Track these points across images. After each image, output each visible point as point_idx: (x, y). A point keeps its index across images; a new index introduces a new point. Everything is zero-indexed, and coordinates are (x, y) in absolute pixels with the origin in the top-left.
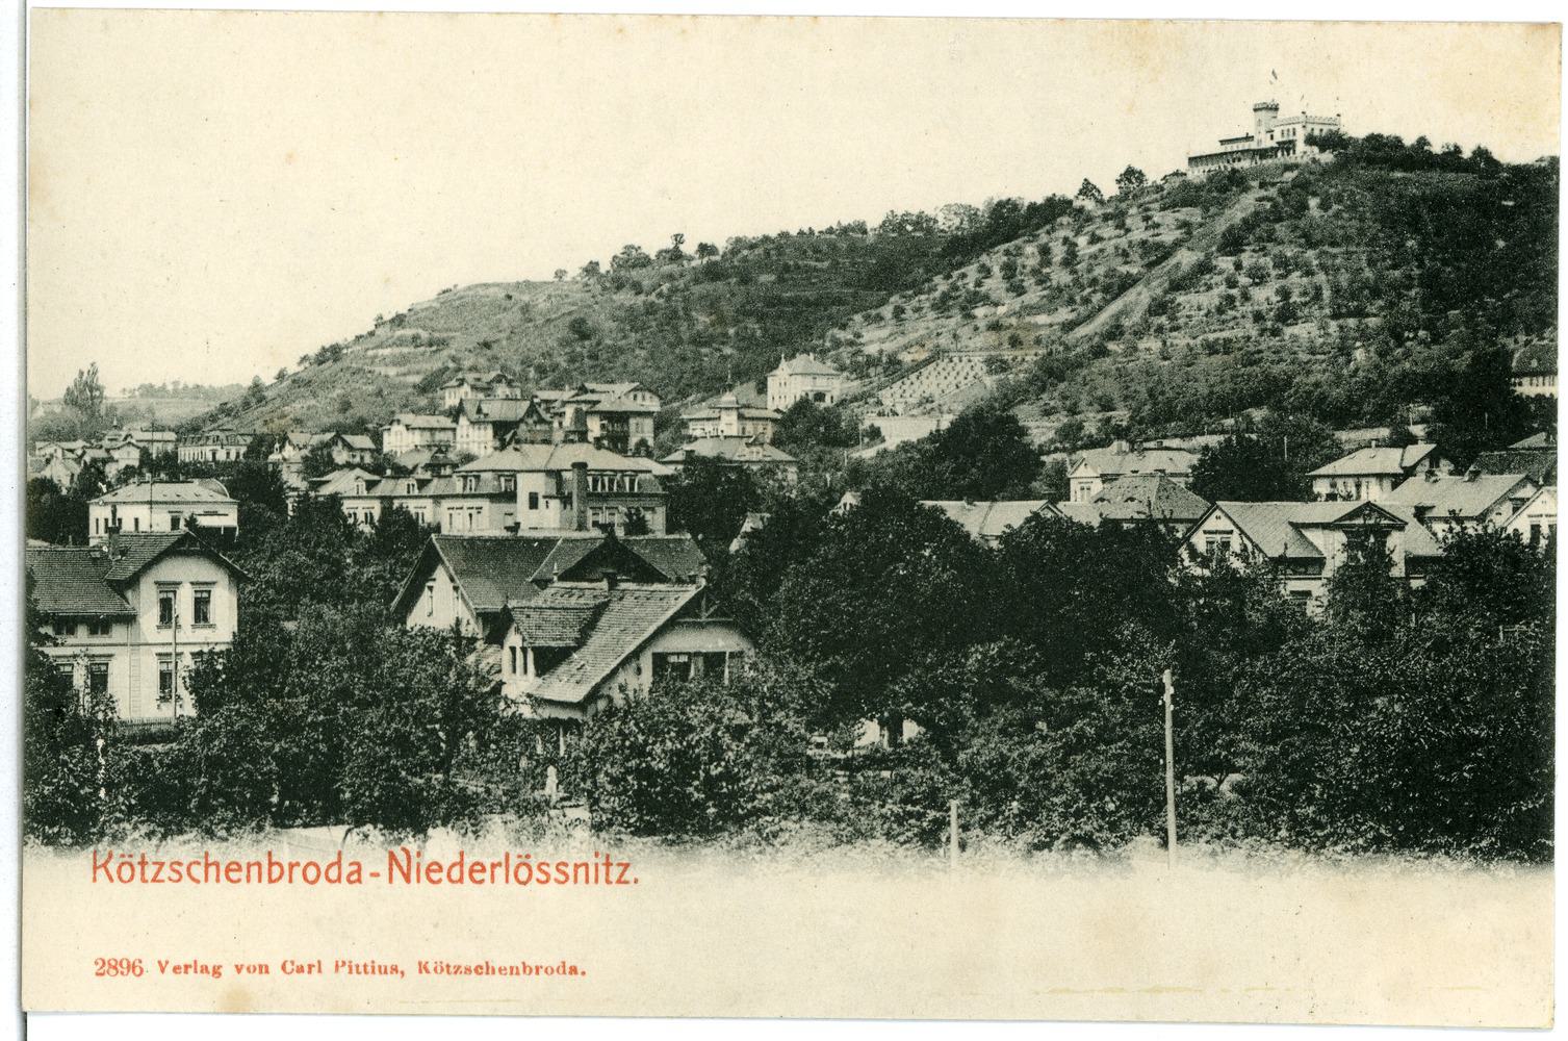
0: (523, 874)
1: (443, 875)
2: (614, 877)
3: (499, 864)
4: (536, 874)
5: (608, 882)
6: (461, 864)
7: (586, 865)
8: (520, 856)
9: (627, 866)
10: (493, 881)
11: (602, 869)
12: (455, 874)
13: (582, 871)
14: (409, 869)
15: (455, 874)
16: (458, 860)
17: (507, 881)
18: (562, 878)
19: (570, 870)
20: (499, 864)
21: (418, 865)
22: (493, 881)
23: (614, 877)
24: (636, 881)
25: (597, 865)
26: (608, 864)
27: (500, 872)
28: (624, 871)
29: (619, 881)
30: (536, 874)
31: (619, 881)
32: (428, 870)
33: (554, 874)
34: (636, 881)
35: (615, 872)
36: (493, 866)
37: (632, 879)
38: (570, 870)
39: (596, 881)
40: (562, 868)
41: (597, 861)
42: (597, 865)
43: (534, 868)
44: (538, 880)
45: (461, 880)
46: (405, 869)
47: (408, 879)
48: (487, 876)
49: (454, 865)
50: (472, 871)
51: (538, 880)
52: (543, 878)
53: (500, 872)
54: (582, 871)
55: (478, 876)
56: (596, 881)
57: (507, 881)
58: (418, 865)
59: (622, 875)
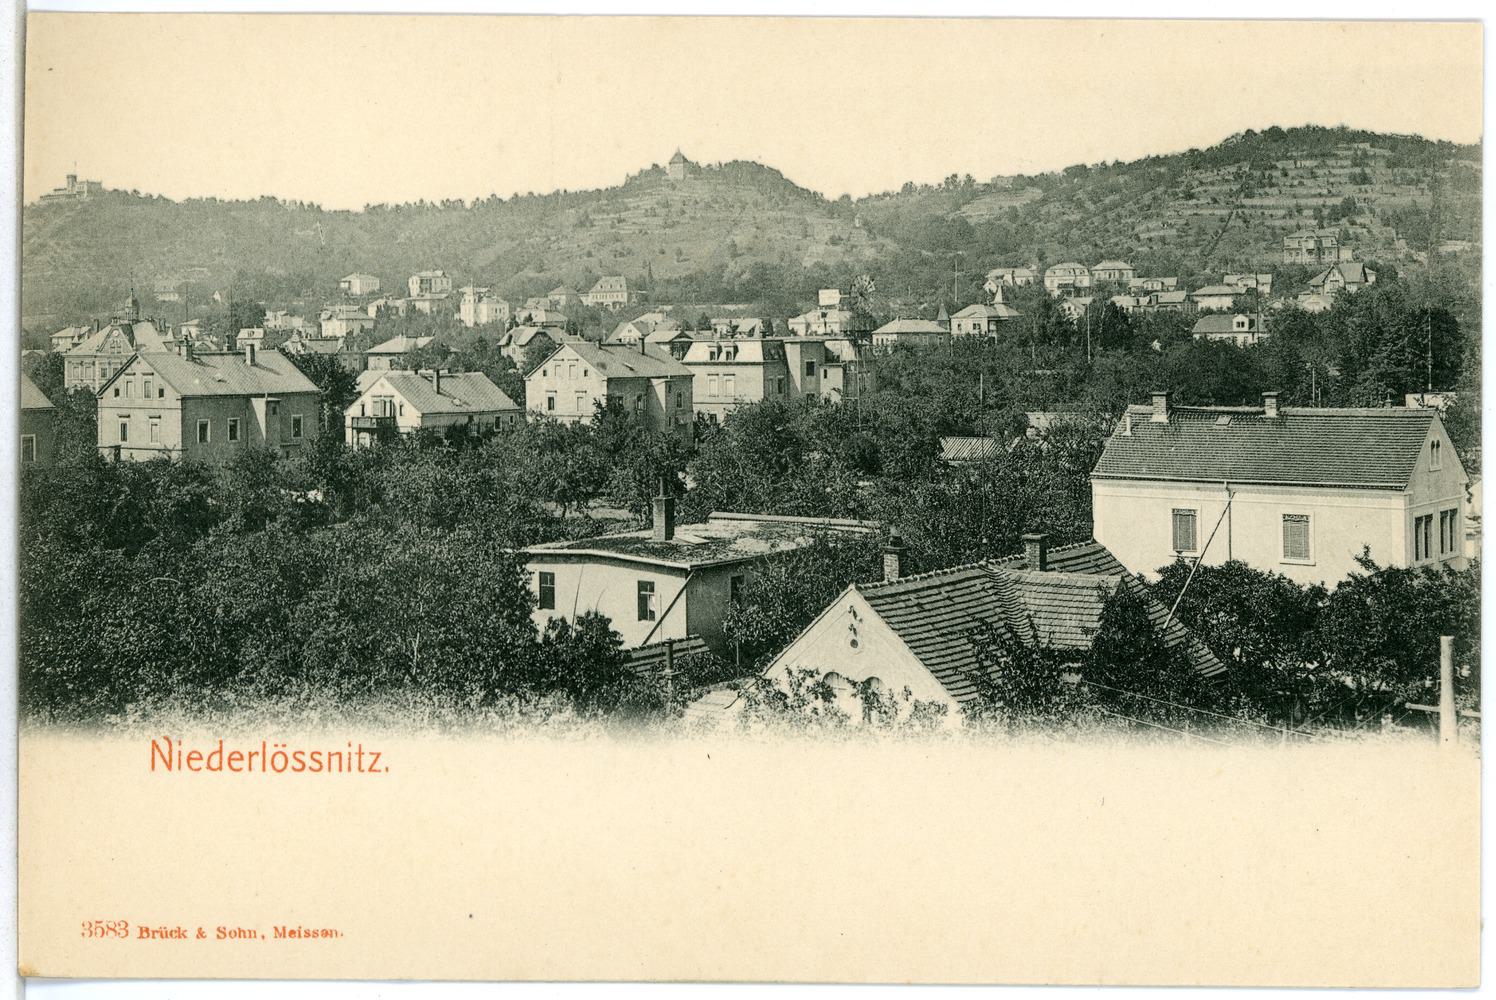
0: (280, 762)
1: (203, 764)
2: (366, 765)
3: (257, 753)
4: (292, 762)
5: (360, 768)
6: (221, 751)
7: (340, 754)
8: (276, 746)
9: (378, 755)
10: (250, 769)
11: (355, 758)
12: (215, 762)
13: (335, 759)
14: (171, 760)
15: (215, 762)
16: (217, 748)
17: (264, 770)
18: (317, 766)
19: (324, 759)
20: (257, 753)
21: (180, 753)
22: (250, 769)
23: (366, 765)
24: (387, 769)
25: (350, 754)
26: (360, 754)
27: (257, 760)
28: (375, 761)
29: (371, 770)
30: (292, 762)
31: (371, 770)
32: (189, 759)
33: (309, 762)
34: (387, 769)
35: (367, 761)
36: (251, 755)
37: (383, 769)
38: (324, 759)
39: (349, 769)
40: (316, 756)
41: (349, 749)
42: (350, 754)
43: (290, 756)
44: (294, 769)
45: (220, 768)
46: (167, 759)
47: (169, 767)
48: (244, 764)
49: (214, 753)
50: (230, 759)
51: (294, 769)
52: (299, 766)
53: (257, 760)
54: (335, 759)
55: (235, 764)
56: (349, 769)
57: (264, 770)
58: (180, 753)
59: (375, 761)
